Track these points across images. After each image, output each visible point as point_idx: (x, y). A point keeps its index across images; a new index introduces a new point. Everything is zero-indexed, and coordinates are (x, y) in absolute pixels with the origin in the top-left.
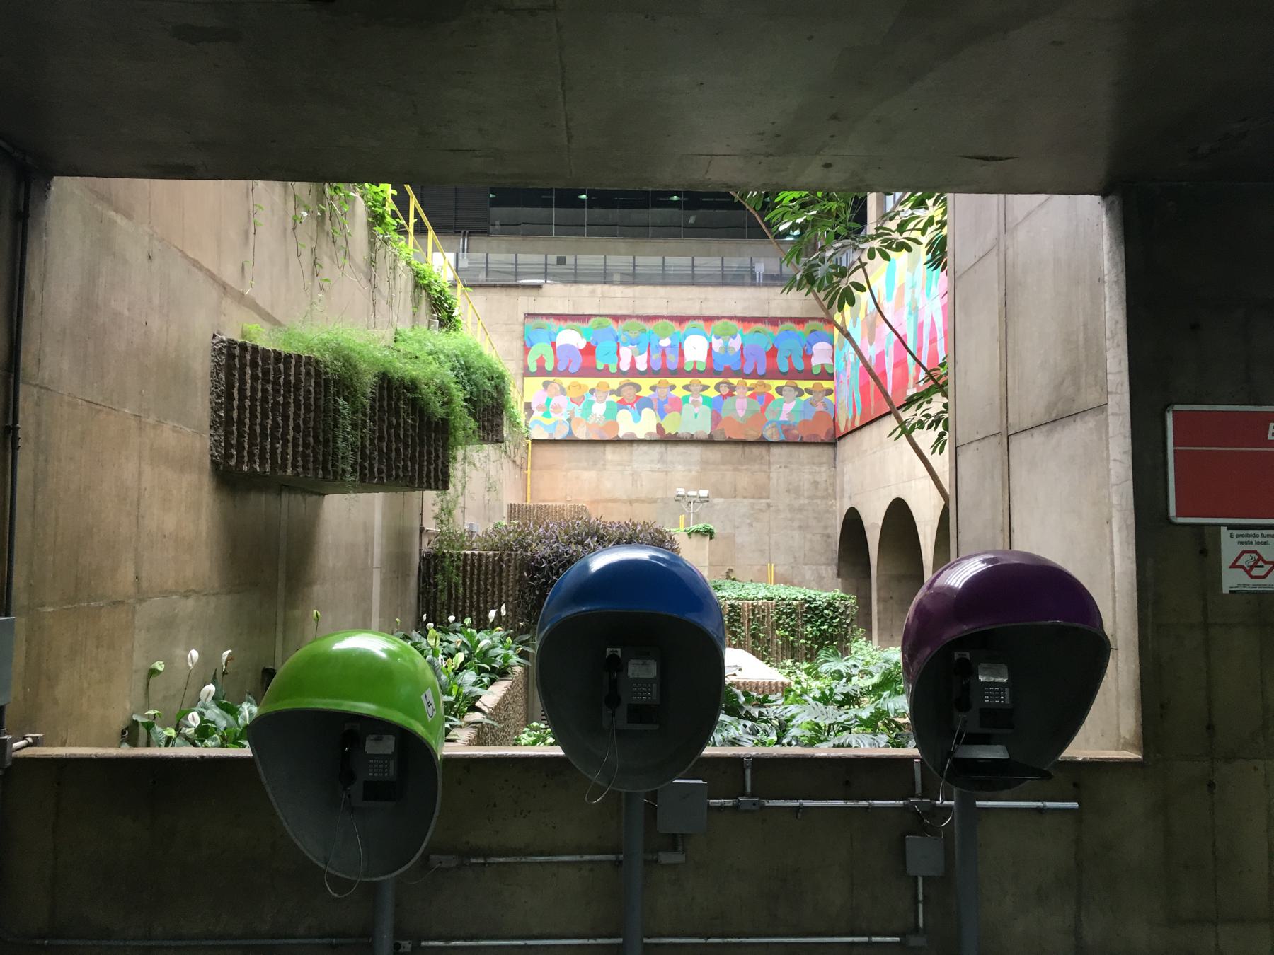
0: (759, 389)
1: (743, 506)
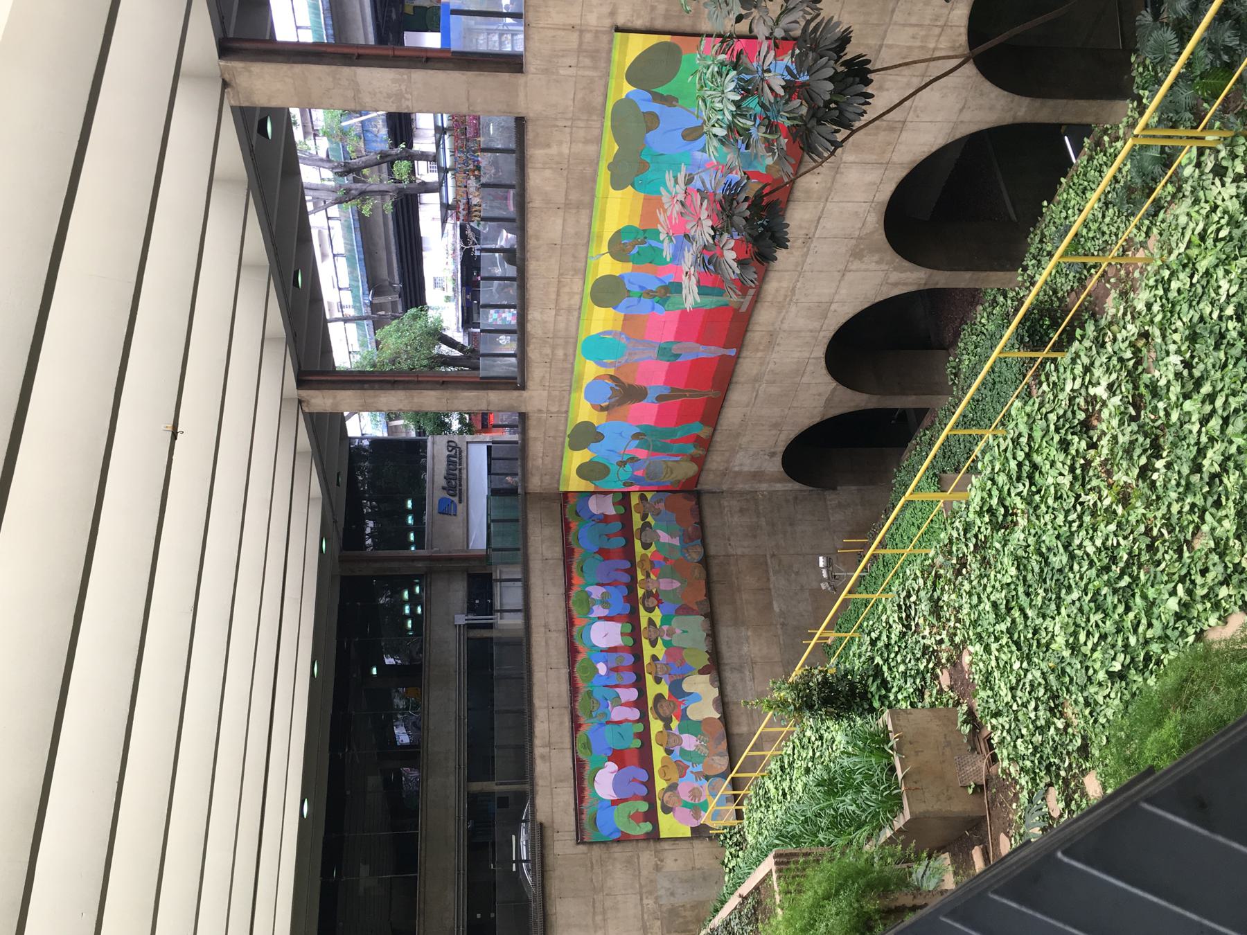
0: (647, 566)
1: (777, 582)
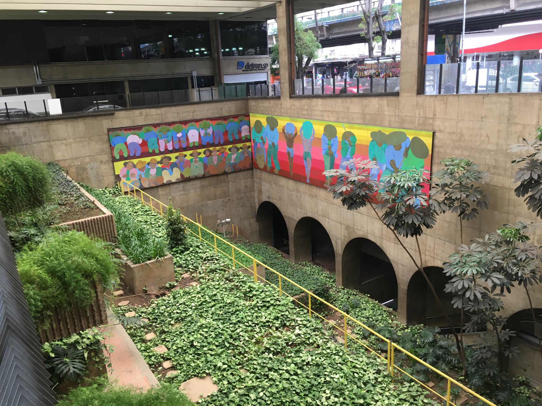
0: (222, 151)
1: (219, 201)
